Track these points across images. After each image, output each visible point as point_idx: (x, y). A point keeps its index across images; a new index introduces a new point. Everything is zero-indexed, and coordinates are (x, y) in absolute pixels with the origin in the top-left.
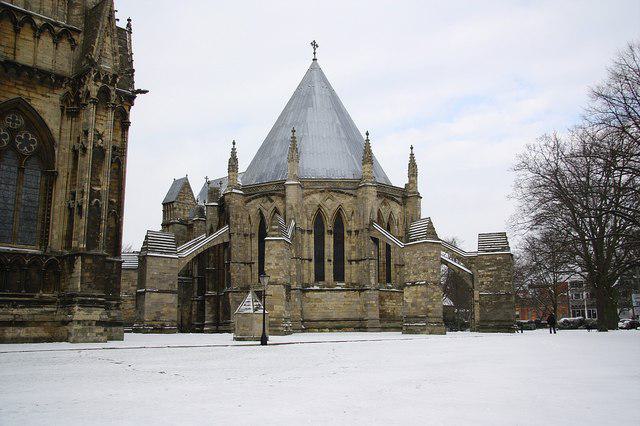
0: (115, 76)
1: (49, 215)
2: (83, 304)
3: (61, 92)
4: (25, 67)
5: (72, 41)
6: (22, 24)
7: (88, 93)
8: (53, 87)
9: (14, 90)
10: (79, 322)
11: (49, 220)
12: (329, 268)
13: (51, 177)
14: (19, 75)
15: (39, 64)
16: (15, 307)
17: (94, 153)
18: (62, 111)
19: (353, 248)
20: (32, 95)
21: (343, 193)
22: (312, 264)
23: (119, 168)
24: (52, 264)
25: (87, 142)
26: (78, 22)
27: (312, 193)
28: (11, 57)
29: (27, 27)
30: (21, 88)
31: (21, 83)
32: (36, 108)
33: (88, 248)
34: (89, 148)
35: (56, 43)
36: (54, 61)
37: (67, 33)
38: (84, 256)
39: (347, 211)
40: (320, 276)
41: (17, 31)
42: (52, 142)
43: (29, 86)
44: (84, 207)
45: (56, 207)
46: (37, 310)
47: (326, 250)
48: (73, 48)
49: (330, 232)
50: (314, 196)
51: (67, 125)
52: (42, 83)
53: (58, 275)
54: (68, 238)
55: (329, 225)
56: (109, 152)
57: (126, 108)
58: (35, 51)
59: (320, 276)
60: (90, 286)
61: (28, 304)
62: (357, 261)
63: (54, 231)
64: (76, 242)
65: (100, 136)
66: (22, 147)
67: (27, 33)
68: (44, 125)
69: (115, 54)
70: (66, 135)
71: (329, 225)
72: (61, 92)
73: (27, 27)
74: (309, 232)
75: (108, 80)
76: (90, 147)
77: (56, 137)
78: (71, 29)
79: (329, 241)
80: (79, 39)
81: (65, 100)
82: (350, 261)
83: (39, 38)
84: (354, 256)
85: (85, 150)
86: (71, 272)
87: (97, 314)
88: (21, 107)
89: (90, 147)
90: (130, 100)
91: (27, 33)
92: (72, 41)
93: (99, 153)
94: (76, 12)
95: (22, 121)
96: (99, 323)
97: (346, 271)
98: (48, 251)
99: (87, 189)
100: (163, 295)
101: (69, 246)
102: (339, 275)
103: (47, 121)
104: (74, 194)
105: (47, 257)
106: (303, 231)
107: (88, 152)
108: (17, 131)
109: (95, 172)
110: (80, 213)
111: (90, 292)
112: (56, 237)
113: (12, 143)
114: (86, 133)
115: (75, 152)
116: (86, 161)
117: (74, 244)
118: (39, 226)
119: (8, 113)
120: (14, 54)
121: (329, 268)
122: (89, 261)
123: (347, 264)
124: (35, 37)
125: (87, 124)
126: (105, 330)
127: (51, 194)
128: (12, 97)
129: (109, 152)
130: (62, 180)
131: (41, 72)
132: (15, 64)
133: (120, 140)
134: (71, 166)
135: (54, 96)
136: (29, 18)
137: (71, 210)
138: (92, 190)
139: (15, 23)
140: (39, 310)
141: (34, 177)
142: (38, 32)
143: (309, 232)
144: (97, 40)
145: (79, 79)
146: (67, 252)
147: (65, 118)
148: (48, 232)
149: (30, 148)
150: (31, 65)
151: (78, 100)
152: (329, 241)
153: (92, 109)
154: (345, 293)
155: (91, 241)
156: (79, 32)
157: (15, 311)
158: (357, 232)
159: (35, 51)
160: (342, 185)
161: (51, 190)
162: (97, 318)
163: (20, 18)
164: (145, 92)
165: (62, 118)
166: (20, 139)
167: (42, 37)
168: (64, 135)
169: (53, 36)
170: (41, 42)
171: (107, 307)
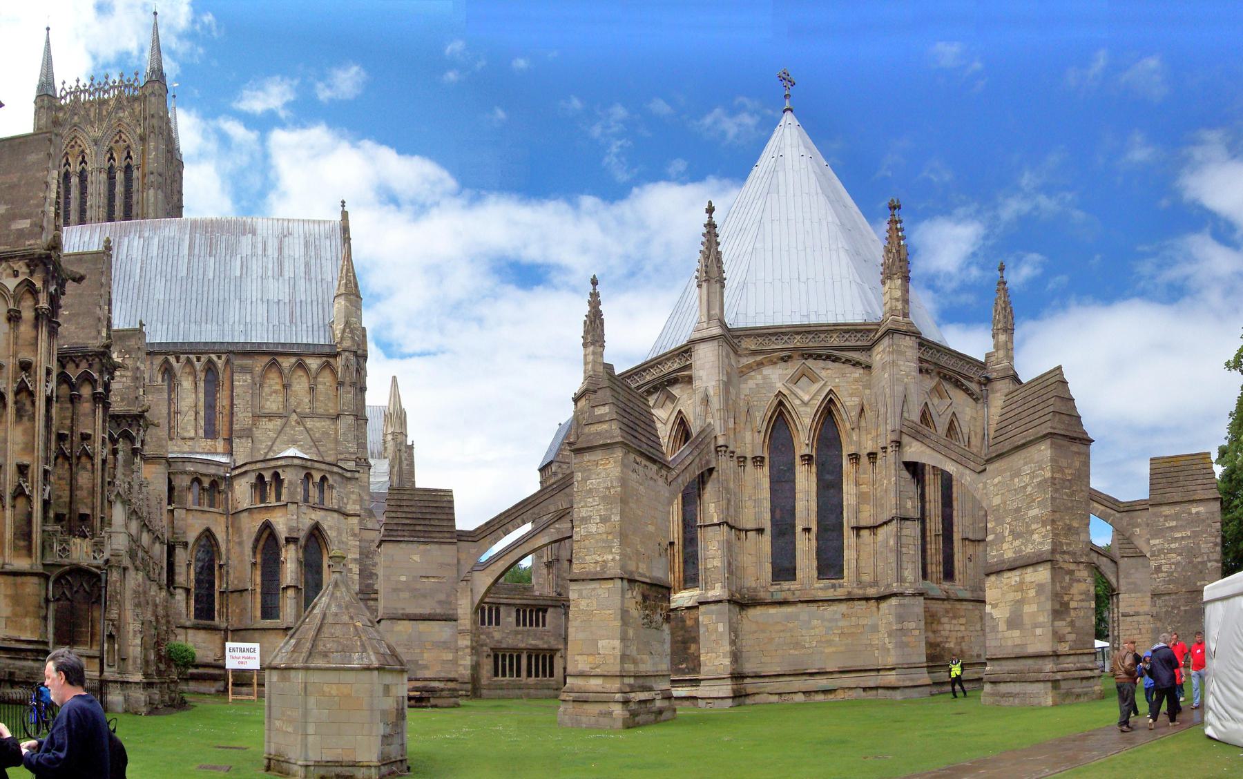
12: (805, 548)
19: (862, 498)
21: (836, 359)
22: (767, 538)
27: (760, 364)
39: (848, 402)
40: (784, 570)
47: (800, 506)
49: (808, 459)
50: (767, 371)
55: (803, 443)
59: (784, 570)
62: (874, 528)
71: (803, 443)
74: (758, 461)
79: (805, 481)
82: (857, 529)
84: (866, 518)
97: (849, 555)
100: (423, 626)
102: (830, 565)
106: (742, 460)
121: (805, 548)
123: (849, 537)
143: (758, 461)
152: (805, 481)
154: (843, 607)
158: (872, 456)
160: (835, 341)
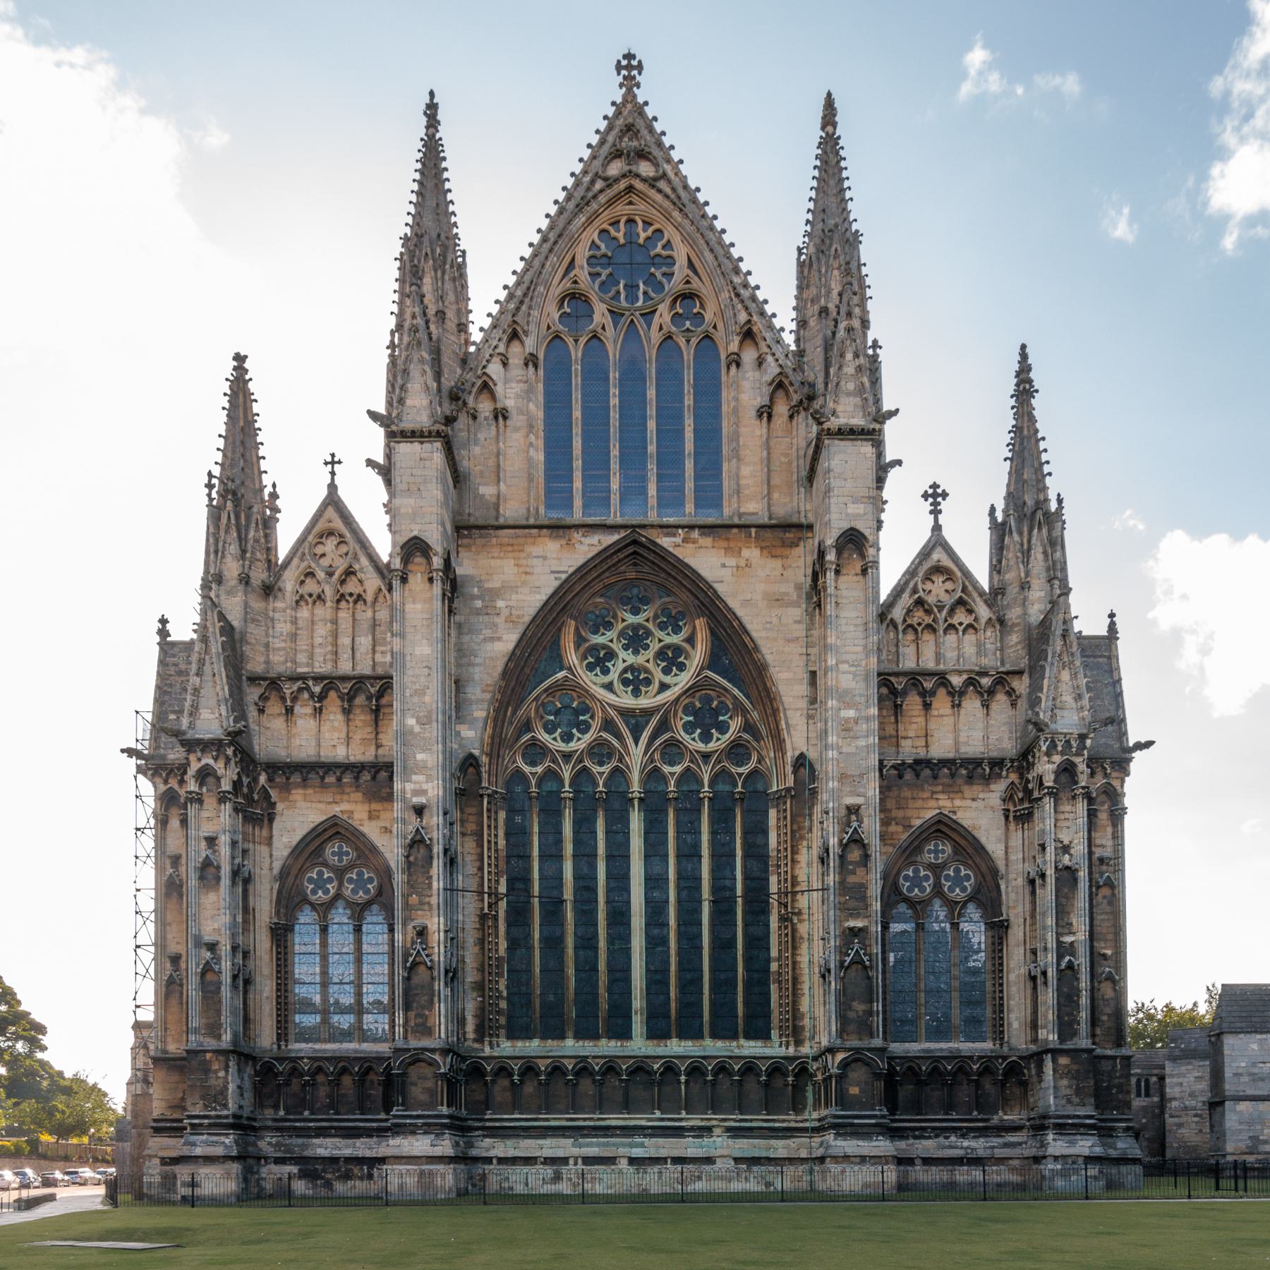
0: (1082, 737)
1: (1001, 991)
2: (1061, 1129)
3: (1000, 787)
4: (944, 762)
5: (1010, 692)
6: (933, 693)
7: (1040, 778)
8: (987, 780)
9: (932, 803)
10: (1056, 1158)
11: (1001, 998)
13: (998, 929)
14: (935, 777)
15: (963, 750)
16: (963, 1136)
17: (1057, 879)
18: (1007, 817)
20: (958, 803)
23: (1113, 895)
24: (1014, 1070)
25: (1045, 862)
26: (1016, 653)
28: (922, 753)
29: (942, 692)
30: (941, 796)
31: (940, 788)
32: (965, 823)
33: (1062, 1039)
34: (1048, 873)
35: (985, 705)
36: (986, 738)
37: (1002, 680)
38: (1055, 1052)
41: (927, 706)
42: (995, 872)
43: (951, 790)
44: (1050, 974)
45: (1012, 977)
46: (996, 1141)
48: (1014, 705)
51: (1017, 838)
52: (970, 779)
53: (1024, 1085)
54: (1034, 1026)
56: (1083, 874)
57: (1116, 783)
58: (956, 730)
60: (1069, 1101)
61: (983, 1132)
63: (1012, 1016)
64: (1045, 1031)
65: (1066, 849)
66: (951, 889)
67: (942, 703)
68: (980, 849)
69: (1079, 697)
70: (1016, 856)
72: (1000, 787)
73: (942, 692)
75: (1071, 747)
76: (1050, 872)
77: (1001, 864)
78: (1008, 673)
80: (1021, 685)
81: (1008, 798)
83: (959, 705)
85: (1043, 876)
86: (1041, 1081)
87: (1086, 1145)
88: (943, 827)
89: (1050, 872)
90: (1121, 764)
91: (942, 703)
92: (1010, 692)
93: (1067, 876)
94: (1014, 638)
95: (949, 849)
96: (1089, 1160)
98: (1005, 1049)
99: (1051, 942)
101: (1035, 1040)
103: (983, 840)
104: (1034, 952)
105: (1004, 1058)
107: (1048, 880)
108: (944, 866)
109: (1062, 912)
110: (1046, 983)
111: (1070, 1110)
112: (1015, 1025)
113: (938, 891)
114: (1043, 847)
115: (1032, 882)
116: (1047, 894)
117: (1042, 1034)
118: (989, 1012)
119: (927, 840)
120: (927, 746)
122: (1063, 1060)
124: (953, 706)
125: (1043, 832)
126: (1101, 1172)
127: (1001, 958)
128: (929, 814)
129: (1083, 874)
130: (1016, 933)
131: (976, 763)
132: (927, 763)
133: (1110, 843)
134: (1028, 907)
135: (991, 795)
136: (942, 679)
137: (1033, 979)
138: (1059, 943)
139: (924, 694)
140: (1000, 1140)
141: (975, 929)
142: (957, 696)
144: (1046, 682)
145: (1025, 758)
146: (1033, 1048)
147: (1012, 826)
148: (1002, 1019)
149: (964, 889)
150: (951, 755)
151: (1028, 793)
153: (1048, 804)
155: (1066, 1027)
156: (1019, 673)
157: (966, 1143)
159: (956, 730)
161: (1001, 950)
162: (1086, 1152)
163: (928, 685)
164: (1149, 744)
165: (1007, 829)
166: (947, 878)
167: (964, 704)
168: (1012, 857)
169: (981, 694)
170: (963, 712)
171: (1104, 1131)
